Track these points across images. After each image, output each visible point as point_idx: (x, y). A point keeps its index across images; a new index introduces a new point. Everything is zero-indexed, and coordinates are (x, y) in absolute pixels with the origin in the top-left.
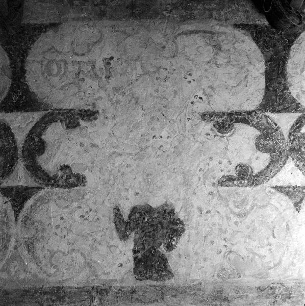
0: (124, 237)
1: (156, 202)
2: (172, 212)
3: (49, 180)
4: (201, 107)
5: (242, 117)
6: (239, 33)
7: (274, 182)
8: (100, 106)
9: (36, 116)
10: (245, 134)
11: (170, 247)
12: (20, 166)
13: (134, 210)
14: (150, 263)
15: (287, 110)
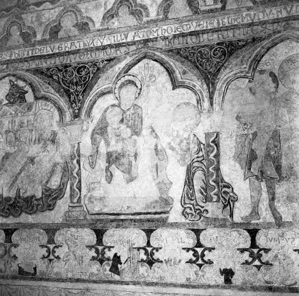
0: (222, 275)
1: (228, 268)
2: (232, 270)
4: (237, 247)
6: (245, 231)
7: (253, 264)
8: (216, 247)
9: (203, 249)
10: (247, 254)
11: (232, 277)
12: (200, 259)
13: (224, 269)
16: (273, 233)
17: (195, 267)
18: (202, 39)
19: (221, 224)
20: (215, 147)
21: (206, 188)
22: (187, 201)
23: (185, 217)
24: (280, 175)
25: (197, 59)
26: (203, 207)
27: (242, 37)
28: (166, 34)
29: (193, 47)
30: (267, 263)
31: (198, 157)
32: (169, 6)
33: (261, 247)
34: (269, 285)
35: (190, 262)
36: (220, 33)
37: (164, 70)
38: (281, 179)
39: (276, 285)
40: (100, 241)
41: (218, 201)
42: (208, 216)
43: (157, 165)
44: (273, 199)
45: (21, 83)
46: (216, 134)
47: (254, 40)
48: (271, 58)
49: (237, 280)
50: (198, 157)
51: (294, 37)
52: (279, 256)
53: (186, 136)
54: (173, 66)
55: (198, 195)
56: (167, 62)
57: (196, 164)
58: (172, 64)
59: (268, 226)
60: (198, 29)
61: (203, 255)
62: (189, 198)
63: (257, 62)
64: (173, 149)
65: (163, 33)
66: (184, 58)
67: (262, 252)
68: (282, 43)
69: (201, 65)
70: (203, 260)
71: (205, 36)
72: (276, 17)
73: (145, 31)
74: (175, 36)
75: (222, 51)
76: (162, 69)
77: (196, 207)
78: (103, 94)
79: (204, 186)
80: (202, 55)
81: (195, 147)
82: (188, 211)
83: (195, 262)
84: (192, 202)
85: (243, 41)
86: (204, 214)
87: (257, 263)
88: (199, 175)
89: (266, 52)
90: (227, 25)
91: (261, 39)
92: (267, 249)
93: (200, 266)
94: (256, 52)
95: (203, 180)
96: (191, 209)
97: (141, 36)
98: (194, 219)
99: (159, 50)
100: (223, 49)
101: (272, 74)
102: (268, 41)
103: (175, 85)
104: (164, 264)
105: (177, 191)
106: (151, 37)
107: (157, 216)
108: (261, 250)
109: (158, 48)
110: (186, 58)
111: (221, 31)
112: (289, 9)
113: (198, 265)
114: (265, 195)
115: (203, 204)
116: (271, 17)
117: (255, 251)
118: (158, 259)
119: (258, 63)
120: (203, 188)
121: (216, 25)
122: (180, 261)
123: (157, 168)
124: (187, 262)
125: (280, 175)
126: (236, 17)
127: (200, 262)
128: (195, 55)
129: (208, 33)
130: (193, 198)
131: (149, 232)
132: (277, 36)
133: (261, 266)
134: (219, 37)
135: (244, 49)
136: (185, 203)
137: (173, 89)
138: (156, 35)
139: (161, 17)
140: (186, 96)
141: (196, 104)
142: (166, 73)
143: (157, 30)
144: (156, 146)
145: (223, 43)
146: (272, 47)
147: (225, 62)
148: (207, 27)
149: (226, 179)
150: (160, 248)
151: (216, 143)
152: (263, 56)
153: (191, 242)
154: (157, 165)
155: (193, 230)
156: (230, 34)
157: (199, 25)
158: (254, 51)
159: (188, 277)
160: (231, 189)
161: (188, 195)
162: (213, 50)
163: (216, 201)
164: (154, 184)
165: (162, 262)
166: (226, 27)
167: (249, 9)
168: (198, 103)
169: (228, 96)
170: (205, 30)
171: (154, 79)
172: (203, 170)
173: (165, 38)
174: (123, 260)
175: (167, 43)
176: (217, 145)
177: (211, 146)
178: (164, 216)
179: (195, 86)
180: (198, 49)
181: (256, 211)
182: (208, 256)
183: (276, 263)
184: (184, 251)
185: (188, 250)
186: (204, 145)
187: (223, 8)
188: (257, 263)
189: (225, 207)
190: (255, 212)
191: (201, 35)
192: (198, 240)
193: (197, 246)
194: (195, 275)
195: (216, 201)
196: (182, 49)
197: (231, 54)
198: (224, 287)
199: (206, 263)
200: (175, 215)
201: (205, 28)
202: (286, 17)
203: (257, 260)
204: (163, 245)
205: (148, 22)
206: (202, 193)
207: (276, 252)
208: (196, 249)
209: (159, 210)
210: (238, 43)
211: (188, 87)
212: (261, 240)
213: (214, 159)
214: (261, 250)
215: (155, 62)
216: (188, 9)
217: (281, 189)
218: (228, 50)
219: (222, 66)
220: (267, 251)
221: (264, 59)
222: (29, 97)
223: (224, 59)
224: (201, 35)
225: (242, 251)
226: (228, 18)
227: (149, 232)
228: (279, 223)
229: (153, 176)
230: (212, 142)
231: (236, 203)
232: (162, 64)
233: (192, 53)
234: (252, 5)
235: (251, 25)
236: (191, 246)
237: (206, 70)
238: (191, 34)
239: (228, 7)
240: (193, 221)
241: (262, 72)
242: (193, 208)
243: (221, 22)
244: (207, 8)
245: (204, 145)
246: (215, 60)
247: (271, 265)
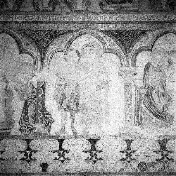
0: (41, 167)
1: (45, 162)
3: (32, 159)
4: (51, 150)
5: (56, 151)
6: (56, 140)
8: (39, 150)
9: (31, 151)
10: (56, 154)
11: (47, 168)
12: (29, 158)
13: (42, 163)
14: (44, 170)
15: (62, 150)
16: (72, 141)
17: (25, 163)
18: (39, 26)
19: (43, 136)
20: (43, 90)
21: (35, 115)
22: (23, 122)
23: (21, 132)
24: (78, 109)
25: (36, 37)
26: (33, 126)
27: (63, 28)
28: (18, 20)
29: (34, 30)
30: (68, 159)
31: (32, 96)
32: (21, 3)
33: (65, 150)
34: (68, 172)
35: (22, 159)
36: (50, 24)
37: (15, 41)
39: (72, 171)
41: (42, 123)
42: (35, 131)
43: (6, 99)
46: (43, 83)
47: (69, 31)
48: (78, 42)
50: (32, 96)
51: (90, 33)
52: (74, 155)
53: (25, 82)
54: (21, 39)
55: (30, 119)
56: (17, 37)
57: (30, 100)
58: (20, 38)
59: (70, 137)
60: (37, 20)
61: (31, 155)
62: (24, 120)
63: (69, 44)
64: (17, 90)
65: (16, 19)
66: (28, 36)
67: (65, 153)
68: (84, 35)
69: (37, 41)
70: (30, 158)
71: (42, 25)
72: (82, 20)
73: (4, 16)
74: (23, 22)
75: (51, 35)
76: (14, 41)
77: (29, 126)
79: (34, 114)
80: (39, 35)
81: (30, 90)
82: (24, 128)
83: (25, 159)
84: (26, 123)
85: (63, 30)
86: (33, 131)
87: (62, 159)
88: (32, 106)
89: (75, 39)
90: (54, 20)
91: (73, 31)
92: (68, 151)
93: (28, 162)
94: (70, 38)
95: (34, 110)
96: (25, 127)
97: (2, 19)
98: (26, 133)
99: (13, 29)
100: (51, 34)
101: (77, 52)
102: (76, 33)
103: (21, 51)
104: (6, 162)
105: (17, 116)
106: (8, 20)
107: (3, 131)
108: (65, 151)
109: (12, 28)
110: (29, 36)
111: (51, 23)
112: (89, 17)
113: (27, 161)
114: (69, 121)
115: (33, 125)
116: (79, 20)
117: (62, 152)
118: (2, 158)
119: (70, 44)
120: (34, 115)
121: (48, 19)
122: (16, 159)
123: (6, 101)
124: (21, 160)
125: (78, 109)
126: (60, 17)
127: (29, 159)
128: (35, 35)
129: (43, 23)
130: (27, 121)
132: (81, 31)
133: (64, 161)
134: (49, 27)
135: (63, 35)
136: (22, 124)
137: (20, 53)
138: (11, 19)
139: (16, 9)
140: (27, 59)
141: (33, 64)
142: (16, 43)
143: (12, 17)
144: (6, 87)
145: (51, 30)
146: (79, 36)
147: (52, 41)
148: (43, 19)
149: (48, 110)
150: (4, 151)
151: (44, 88)
152: (73, 40)
153: (23, 147)
154: (6, 99)
155: (25, 140)
156: (56, 25)
157: (38, 18)
158: (68, 37)
159: (21, 168)
160: (50, 115)
161: (24, 119)
162: (45, 34)
163: (41, 123)
164: (3, 111)
165: (4, 160)
166: (54, 21)
167: (68, 13)
168: (34, 64)
169: (52, 61)
170: (41, 21)
171: (8, 46)
172: (34, 104)
173: (17, 22)
175: (18, 25)
176: (44, 89)
177: (40, 90)
178: (8, 131)
179: (33, 53)
180: (36, 32)
181: (64, 129)
182: (34, 155)
183: (72, 159)
184: (19, 153)
185: (21, 152)
186: (36, 89)
187: (53, 10)
188: (62, 159)
189: (46, 126)
190: (63, 130)
191: (39, 24)
192: (28, 146)
193: (27, 150)
194: (25, 167)
195: (41, 123)
196: (27, 30)
197: (55, 37)
198: (42, 174)
199: (32, 159)
200: (15, 131)
201: (41, 20)
202: (87, 21)
203: (62, 157)
204: (6, 149)
205: (7, 11)
206: (33, 118)
207: (73, 152)
208: (27, 151)
209: (5, 128)
210: (60, 32)
211: (29, 54)
212: (65, 146)
213: (41, 97)
214: (65, 151)
215: (9, 36)
216: (32, 7)
217: (78, 117)
218: (54, 35)
219: (50, 43)
220: (68, 152)
221: (73, 43)
223: (51, 40)
224: (39, 24)
225: (54, 152)
226: (55, 16)
228: (76, 136)
229: (3, 106)
230: (41, 87)
231: (52, 124)
232: (14, 38)
233: (33, 33)
234: (69, 11)
235: (68, 22)
236: (23, 150)
237: (40, 44)
238: (33, 22)
239: (56, 10)
240: (26, 134)
241: (72, 50)
242: (26, 127)
243: (51, 18)
244: (44, 9)
245: (36, 89)
246: (46, 40)
247: (70, 160)
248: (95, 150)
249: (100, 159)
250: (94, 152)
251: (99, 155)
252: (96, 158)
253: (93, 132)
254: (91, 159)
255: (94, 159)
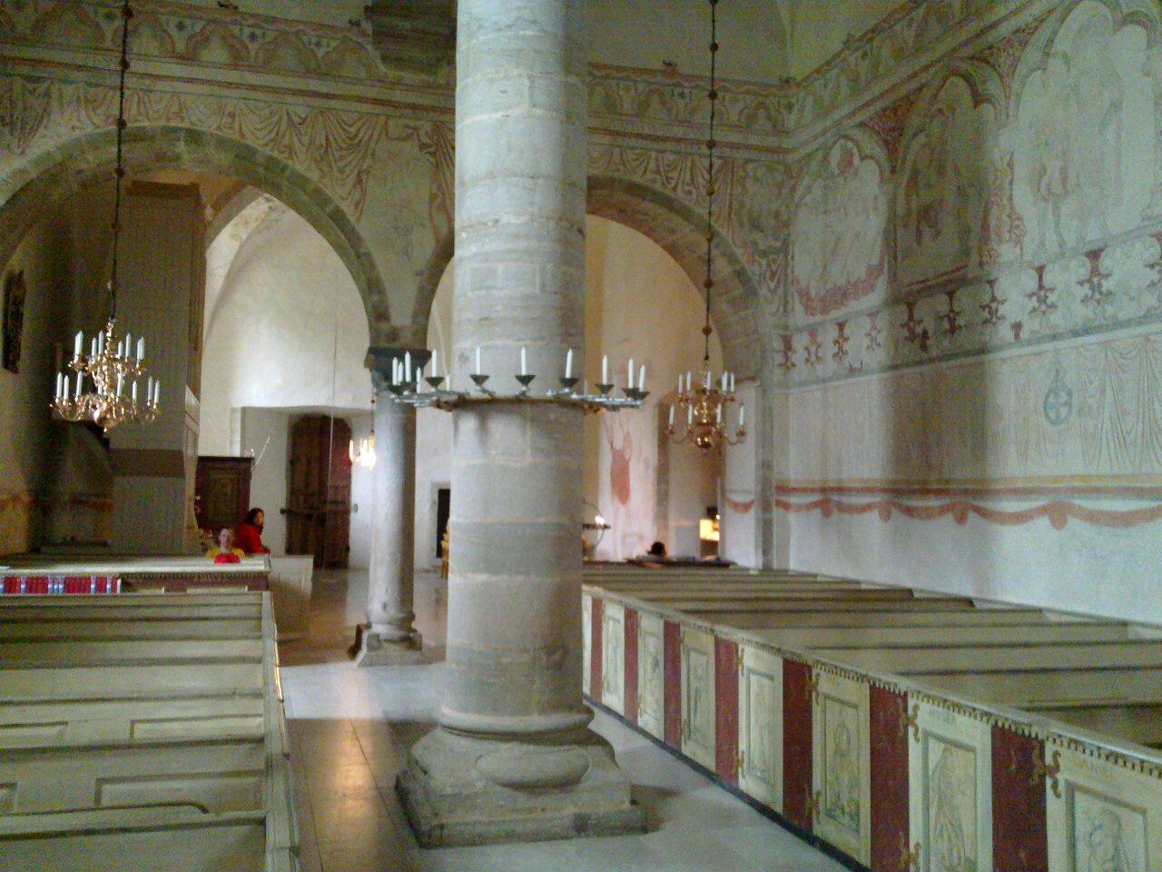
38: (1067, 192)
40: (911, 317)
44: (1057, 224)
45: (850, 145)
49: (1024, 335)
78: (915, 135)
131: (951, 295)
151: (1010, 165)
174: (930, 333)
212: (1048, 279)
217: (1069, 206)
222: (856, 160)
227: (951, 295)
248: (1099, 275)
249: (1110, 293)
250: (1096, 280)
251: (1107, 285)
252: (1101, 293)
253: (1093, 236)
254: (1092, 298)
255: (1097, 296)
